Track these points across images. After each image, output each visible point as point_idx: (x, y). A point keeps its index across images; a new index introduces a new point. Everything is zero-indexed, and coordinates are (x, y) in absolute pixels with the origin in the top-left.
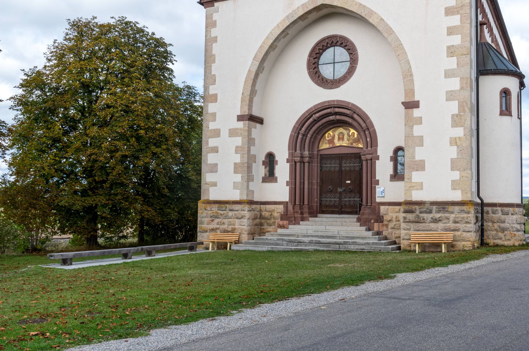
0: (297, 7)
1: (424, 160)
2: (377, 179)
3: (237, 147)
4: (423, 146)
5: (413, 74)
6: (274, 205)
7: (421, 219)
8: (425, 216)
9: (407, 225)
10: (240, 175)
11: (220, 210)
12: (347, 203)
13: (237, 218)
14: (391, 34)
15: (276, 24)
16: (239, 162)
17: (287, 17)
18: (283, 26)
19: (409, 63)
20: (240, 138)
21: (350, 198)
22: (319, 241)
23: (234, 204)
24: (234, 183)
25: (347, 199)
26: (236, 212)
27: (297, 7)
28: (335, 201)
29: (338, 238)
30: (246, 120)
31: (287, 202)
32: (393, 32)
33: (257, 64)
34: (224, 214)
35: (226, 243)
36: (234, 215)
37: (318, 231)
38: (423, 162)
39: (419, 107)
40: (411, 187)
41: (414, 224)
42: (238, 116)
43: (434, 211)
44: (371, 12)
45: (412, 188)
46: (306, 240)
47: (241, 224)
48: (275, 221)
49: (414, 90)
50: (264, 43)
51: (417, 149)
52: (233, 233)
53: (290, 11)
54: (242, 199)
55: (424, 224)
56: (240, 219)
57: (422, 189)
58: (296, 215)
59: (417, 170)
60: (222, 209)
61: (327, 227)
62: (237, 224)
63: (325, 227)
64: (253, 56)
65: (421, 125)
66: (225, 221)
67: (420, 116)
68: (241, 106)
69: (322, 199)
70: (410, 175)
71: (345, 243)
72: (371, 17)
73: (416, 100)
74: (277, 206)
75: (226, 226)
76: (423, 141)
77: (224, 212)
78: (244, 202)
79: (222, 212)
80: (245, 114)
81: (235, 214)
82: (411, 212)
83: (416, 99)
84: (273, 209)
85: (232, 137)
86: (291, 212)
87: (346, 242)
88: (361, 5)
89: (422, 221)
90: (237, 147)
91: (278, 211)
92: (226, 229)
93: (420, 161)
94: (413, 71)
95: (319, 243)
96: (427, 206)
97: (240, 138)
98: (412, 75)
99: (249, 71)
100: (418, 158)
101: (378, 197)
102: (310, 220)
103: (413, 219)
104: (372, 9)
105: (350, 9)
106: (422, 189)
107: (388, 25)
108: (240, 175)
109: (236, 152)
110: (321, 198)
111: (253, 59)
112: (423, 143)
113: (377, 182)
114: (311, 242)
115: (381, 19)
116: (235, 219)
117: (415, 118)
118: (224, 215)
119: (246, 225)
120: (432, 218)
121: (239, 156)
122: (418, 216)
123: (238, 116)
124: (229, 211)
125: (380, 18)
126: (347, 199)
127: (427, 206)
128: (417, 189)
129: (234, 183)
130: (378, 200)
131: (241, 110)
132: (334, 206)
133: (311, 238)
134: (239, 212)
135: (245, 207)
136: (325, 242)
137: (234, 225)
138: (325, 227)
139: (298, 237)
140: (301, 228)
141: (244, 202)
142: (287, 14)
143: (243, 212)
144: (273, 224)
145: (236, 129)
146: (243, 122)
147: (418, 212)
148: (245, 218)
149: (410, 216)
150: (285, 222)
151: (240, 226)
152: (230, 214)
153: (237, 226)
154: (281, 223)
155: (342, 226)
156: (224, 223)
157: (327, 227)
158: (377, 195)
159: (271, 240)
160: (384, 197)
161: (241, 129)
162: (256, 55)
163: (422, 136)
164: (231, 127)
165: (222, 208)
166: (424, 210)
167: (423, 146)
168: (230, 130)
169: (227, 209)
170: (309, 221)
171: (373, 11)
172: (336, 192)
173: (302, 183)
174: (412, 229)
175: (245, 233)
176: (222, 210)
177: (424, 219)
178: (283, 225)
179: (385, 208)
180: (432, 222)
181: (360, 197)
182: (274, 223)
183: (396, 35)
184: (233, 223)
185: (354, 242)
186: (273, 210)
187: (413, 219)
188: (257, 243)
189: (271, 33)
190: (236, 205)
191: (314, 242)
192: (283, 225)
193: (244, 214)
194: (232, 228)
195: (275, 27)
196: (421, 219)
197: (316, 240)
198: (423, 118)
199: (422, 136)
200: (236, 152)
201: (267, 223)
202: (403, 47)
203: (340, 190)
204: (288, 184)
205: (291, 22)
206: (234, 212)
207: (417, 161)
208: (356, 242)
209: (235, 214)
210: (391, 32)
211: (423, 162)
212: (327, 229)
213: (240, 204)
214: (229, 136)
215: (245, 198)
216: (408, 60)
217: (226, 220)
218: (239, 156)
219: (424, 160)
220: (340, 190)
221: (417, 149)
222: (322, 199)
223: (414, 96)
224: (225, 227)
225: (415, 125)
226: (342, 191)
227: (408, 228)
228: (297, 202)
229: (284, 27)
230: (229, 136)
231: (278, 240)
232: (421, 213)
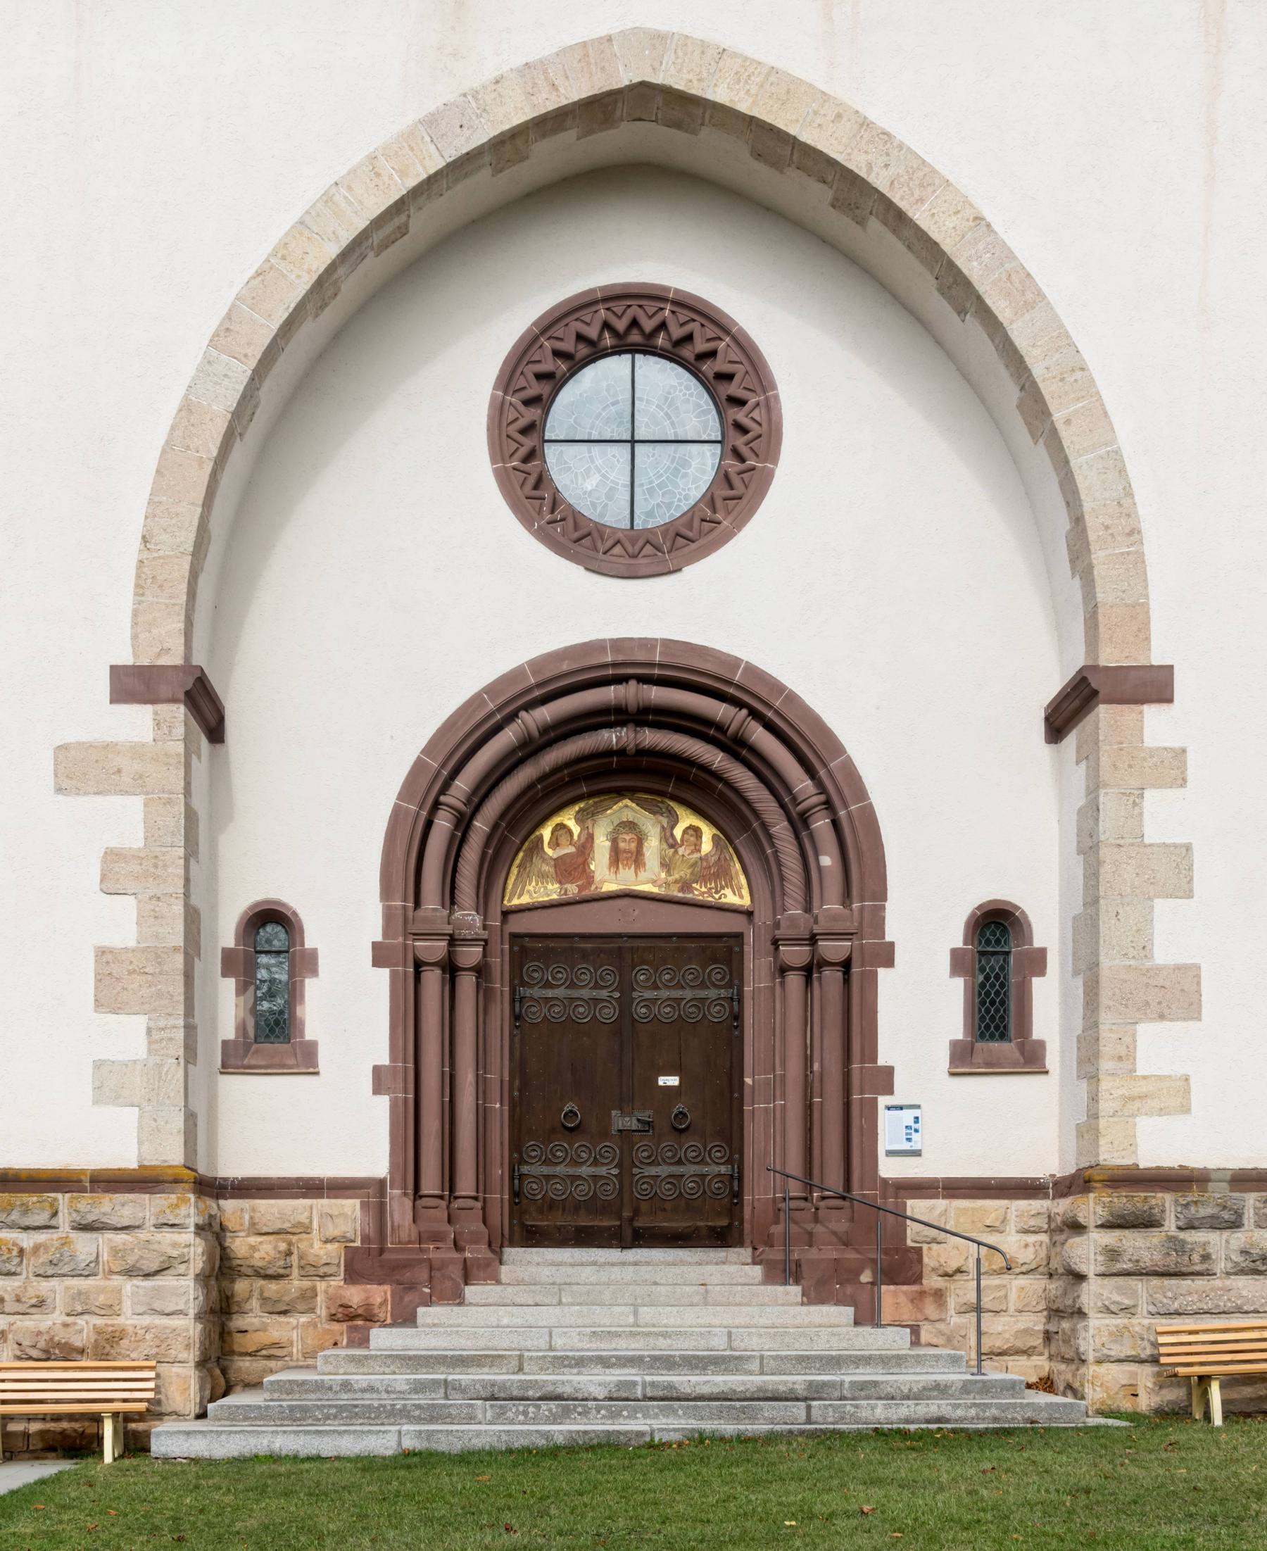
0: (497, 74)
1: (1198, 967)
2: (882, 1061)
3: (112, 857)
4: (1189, 894)
5: (1144, 526)
6: (305, 1196)
7: (1196, 1257)
8: (1214, 1240)
9: (1118, 1289)
10: (138, 1023)
11: (13, 1226)
12: (665, 1190)
13: (130, 1272)
14: (1029, 306)
15: (358, 156)
16: (132, 943)
17: (431, 121)
18: (403, 173)
19: (1122, 471)
20: (135, 804)
21: (680, 1162)
22: (671, 1386)
23: (115, 1191)
24: (98, 1065)
25: (663, 1170)
26: (121, 1238)
27: (490, 75)
28: (595, 1177)
29: (755, 1366)
30: (174, 700)
31: (382, 1182)
32: (1040, 294)
33: (241, 373)
34: (36, 1248)
35: (97, 1419)
36: (105, 1257)
37: (617, 1335)
38: (1191, 973)
39: (1170, 700)
40: (1132, 1099)
41: (1155, 1281)
42: (114, 670)
43: (1249, 1217)
44: (926, 176)
45: (1137, 1104)
46: (594, 1381)
47: (157, 1305)
48: (314, 1289)
49: (1145, 608)
50: (282, 251)
51: (1163, 908)
52: (104, 1356)
53: (444, 93)
54: (152, 1160)
55: (1200, 1283)
56: (147, 1275)
57: (1185, 1109)
58: (433, 1253)
59: (1162, 1017)
60: (28, 1221)
61: (642, 1310)
62: (127, 1306)
63: (636, 1313)
64: (212, 324)
65: (1179, 792)
66: (56, 1289)
67: (1176, 744)
68: (135, 614)
69: (525, 1169)
70: (1127, 1040)
71: (815, 1392)
72: (921, 200)
73: (1155, 663)
74: (324, 1204)
75: (58, 1317)
76: (1190, 869)
77: (41, 1237)
78: (177, 1181)
79: (28, 1240)
80: (165, 661)
81: (115, 1251)
82: (1147, 1222)
83: (1156, 660)
84: (303, 1218)
85: (78, 792)
86: (404, 1236)
87: (824, 1384)
88: (865, 124)
89: (1198, 1268)
90: (112, 857)
91: (332, 1231)
92: (61, 1336)
93: (1179, 968)
94: (1141, 511)
95: (670, 1397)
96: (1218, 1191)
97: (135, 804)
98: (1134, 532)
99: (187, 408)
100: (1164, 954)
101: (890, 1153)
102: (504, 1278)
103: (1157, 1257)
104: (928, 159)
105: (807, 137)
106: (1185, 1109)
107: (1011, 256)
108: (138, 1023)
109: (110, 884)
110: (522, 1161)
111: (213, 343)
112: (1190, 881)
113: (885, 1080)
114: (620, 1398)
115: (978, 219)
116: (117, 1280)
117: (1153, 752)
118: (44, 1258)
119: (192, 1313)
120: (1244, 1252)
121: (126, 908)
122: (1178, 1246)
123: (114, 670)
124: (74, 1235)
125: (969, 213)
126: (663, 1170)
127: (1218, 1191)
128: (1161, 1112)
129: (98, 1065)
130: (889, 1169)
131: (135, 637)
132: (593, 1205)
133: (599, 1369)
134: (142, 1235)
135: (183, 1211)
136: (706, 1390)
137: (111, 1309)
138: (636, 1313)
139: (521, 1370)
140: (493, 1321)
141: (177, 1181)
142: (431, 106)
143: (168, 1236)
144: (300, 1307)
145: (107, 747)
146: (148, 709)
147: (1170, 1225)
148: (182, 1268)
149: (1139, 1245)
150: (379, 1294)
151: (147, 1320)
152: (85, 1246)
153: (127, 1320)
154: (355, 1295)
155: (706, 1304)
156: (40, 1304)
157: (642, 1310)
158: (884, 1144)
159: (371, 1389)
160: (917, 1153)
161: (136, 751)
162: (229, 317)
163: (1188, 848)
164: (73, 735)
165: (26, 1211)
166: (1205, 1211)
167: (1189, 894)
168: (62, 749)
169: (64, 1220)
170: (499, 1282)
171: (934, 171)
172: (605, 1134)
173: (451, 1082)
174: (1144, 1307)
175: (183, 1355)
176: (26, 1228)
177: (1206, 1257)
178: (368, 1306)
179: (932, 1209)
180: (1242, 1272)
181: (729, 1161)
182: (308, 1296)
183: (1056, 317)
184: (101, 1299)
185: (863, 1386)
186: (300, 1224)
187: (1157, 1257)
188: (304, 1409)
189: (327, 198)
190: (119, 1197)
191: (639, 1394)
192: (368, 1306)
193: (175, 1245)
194: (99, 1331)
195: (353, 171)
196: (1196, 1257)
197: (653, 1384)
198: (1190, 756)
199: (1188, 848)
200: (110, 884)
201: (264, 1300)
202: (1092, 382)
203: (622, 1121)
204: (380, 1081)
205: (452, 154)
206: (109, 1235)
207: (1159, 969)
208: (876, 1383)
209: (115, 1251)
210: (1029, 296)
211: (1191, 973)
212: (642, 1321)
213: (143, 1190)
214: (59, 790)
215: (171, 1154)
216: (1117, 452)
217: (54, 1282)
218: (126, 908)
219: (1198, 967)
220: (622, 1121)
221: (1163, 908)
222: (525, 1169)
223: (1148, 639)
224: (50, 1322)
225: (1153, 786)
226: (635, 1125)
227: (1127, 1302)
228: (430, 1184)
229: (412, 182)
230: (59, 790)
231: (419, 1387)
232: (1190, 1226)
